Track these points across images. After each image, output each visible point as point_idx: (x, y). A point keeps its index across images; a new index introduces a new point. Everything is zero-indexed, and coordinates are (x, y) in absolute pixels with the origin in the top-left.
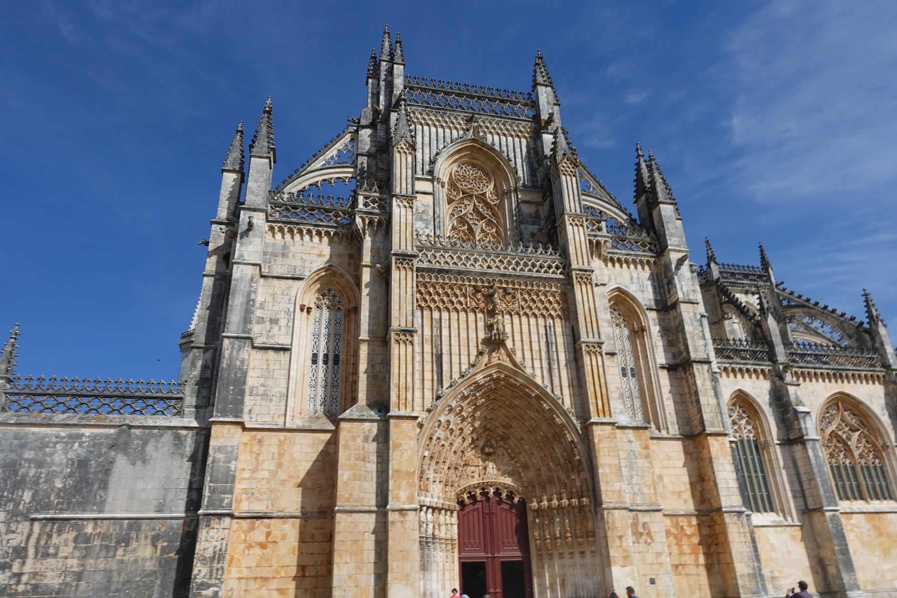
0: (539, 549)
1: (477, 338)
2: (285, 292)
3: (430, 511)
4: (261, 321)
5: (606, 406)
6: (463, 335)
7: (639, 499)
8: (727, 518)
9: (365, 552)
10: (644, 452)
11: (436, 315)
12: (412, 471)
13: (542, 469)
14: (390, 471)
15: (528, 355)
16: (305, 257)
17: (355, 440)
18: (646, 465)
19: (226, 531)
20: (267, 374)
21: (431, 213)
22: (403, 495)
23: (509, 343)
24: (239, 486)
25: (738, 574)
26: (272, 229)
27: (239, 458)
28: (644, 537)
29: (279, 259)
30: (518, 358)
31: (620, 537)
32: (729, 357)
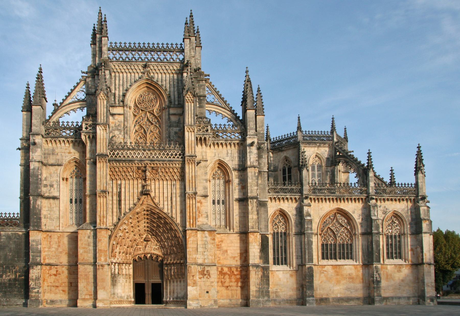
2: (55, 172)
4: (46, 186)
5: (194, 222)
6: (131, 191)
7: (206, 261)
8: (251, 268)
11: (119, 182)
16: (63, 154)
19: (40, 270)
20: (50, 209)
21: (122, 126)
23: (152, 194)
24: (43, 254)
25: (251, 290)
26: (47, 141)
27: (42, 243)
28: (206, 276)
29: (51, 156)
30: (156, 201)
32: (277, 192)
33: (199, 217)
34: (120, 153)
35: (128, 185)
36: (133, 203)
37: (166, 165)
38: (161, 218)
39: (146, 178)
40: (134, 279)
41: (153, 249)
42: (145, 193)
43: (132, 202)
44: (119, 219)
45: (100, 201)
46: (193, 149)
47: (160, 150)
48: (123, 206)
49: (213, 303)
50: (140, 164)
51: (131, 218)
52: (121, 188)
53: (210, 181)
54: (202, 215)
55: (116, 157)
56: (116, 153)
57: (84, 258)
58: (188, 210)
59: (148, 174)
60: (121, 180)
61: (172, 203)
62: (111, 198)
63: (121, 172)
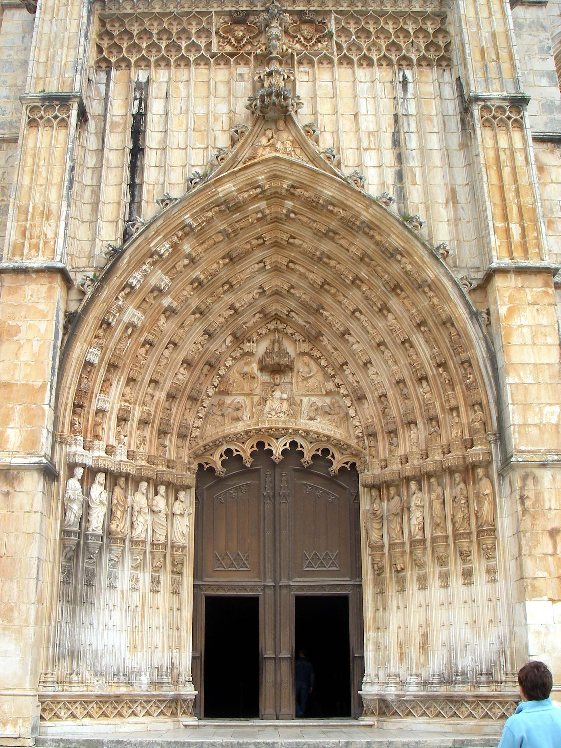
0: (379, 571)
3: (101, 477)
13: (390, 394)
15: (348, 141)
22: (14, 436)
23: (302, 118)
48: (150, 175)
52: (144, 101)
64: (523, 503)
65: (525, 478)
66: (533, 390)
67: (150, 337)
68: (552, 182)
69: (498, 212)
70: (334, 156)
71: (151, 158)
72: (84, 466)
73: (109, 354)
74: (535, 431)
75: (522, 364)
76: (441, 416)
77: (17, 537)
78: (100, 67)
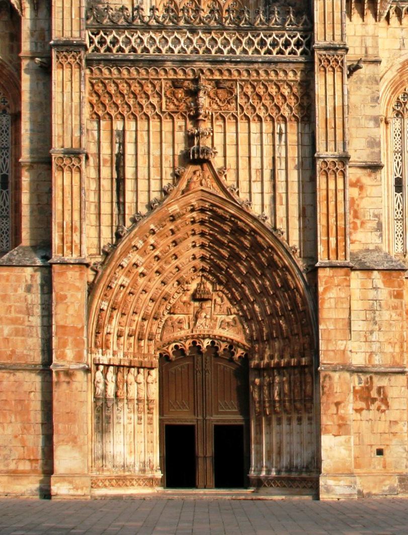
1: (174, 155)
5: (341, 245)
6: (155, 151)
7: (377, 360)
9: (32, 413)
10: (394, 301)
11: (118, 125)
12: (80, 326)
14: (54, 327)
15: (244, 174)
17: (16, 290)
18: (395, 317)
22: (70, 353)
28: (377, 403)
30: (229, 181)
31: (337, 404)
33: (355, 228)
34: (121, 39)
35: (145, 134)
36: (158, 188)
37: (258, 74)
38: (242, 232)
39: (197, 114)
40: (161, 413)
41: (220, 323)
42: (195, 156)
43: (155, 185)
44: (119, 236)
45: (61, 181)
46: (338, 27)
47: (239, 29)
48: (129, 196)
49: (396, 484)
50: (181, 73)
51: (153, 232)
52: (123, 144)
53: (387, 123)
54: (363, 223)
55: (109, 50)
56: (109, 39)
57: (13, 352)
58: (321, 209)
59: (203, 100)
60: (123, 119)
61: (274, 187)
62: (93, 173)
63: (123, 95)
64: (323, 389)
65: (325, 377)
66: (333, 333)
67: (132, 290)
68: (367, 196)
69: (325, 230)
70: (235, 190)
71: (129, 185)
72: (103, 364)
73: (111, 302)
74: (332, 354)
75: (329, 319)
76: (291, 337)
77: (76, 404)
78: (93, 118)
